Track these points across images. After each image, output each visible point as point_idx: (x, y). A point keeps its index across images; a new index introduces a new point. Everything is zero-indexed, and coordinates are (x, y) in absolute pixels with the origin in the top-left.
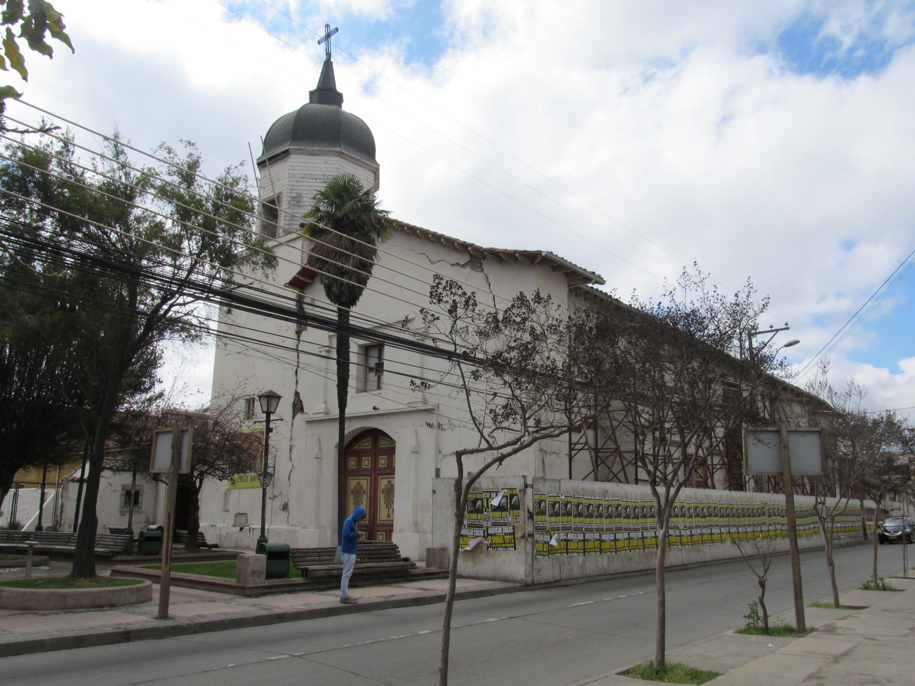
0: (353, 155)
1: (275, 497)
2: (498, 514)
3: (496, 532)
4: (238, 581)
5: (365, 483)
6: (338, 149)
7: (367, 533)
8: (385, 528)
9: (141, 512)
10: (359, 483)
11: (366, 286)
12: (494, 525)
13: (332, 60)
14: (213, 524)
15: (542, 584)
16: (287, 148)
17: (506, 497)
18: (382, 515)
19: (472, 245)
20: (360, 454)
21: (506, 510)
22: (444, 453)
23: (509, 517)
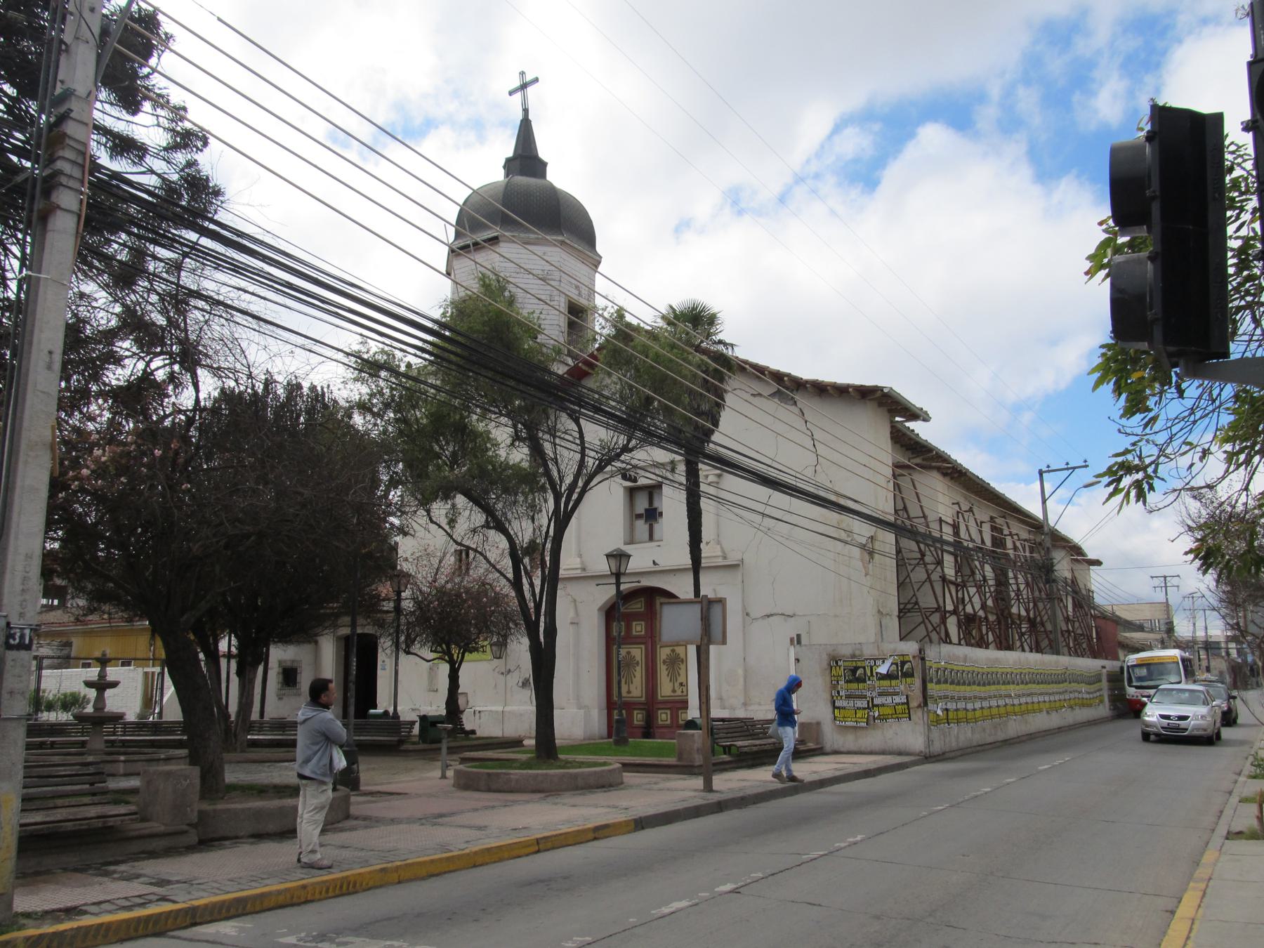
0: (576, 246)
1: (509, 671)
2: (886, 683)
3: (884, 702)
4: (680, 758)
5: (637, 652)
6: (560, 238)
7: (644, 712)
8: (669, 705)
9: (299, 695)
10: (629, 653)
11: (717, 427)
12: (881, 694)
13: (530, 118)
14: (413, 707)
15: (935, 756)
16: (496, 234)
17: (897, 664)
18: (666, 689)
19: (789, 375)
20: (629, 618)
21: (897, 678)
22: (753, 615)
23: (900, 685)
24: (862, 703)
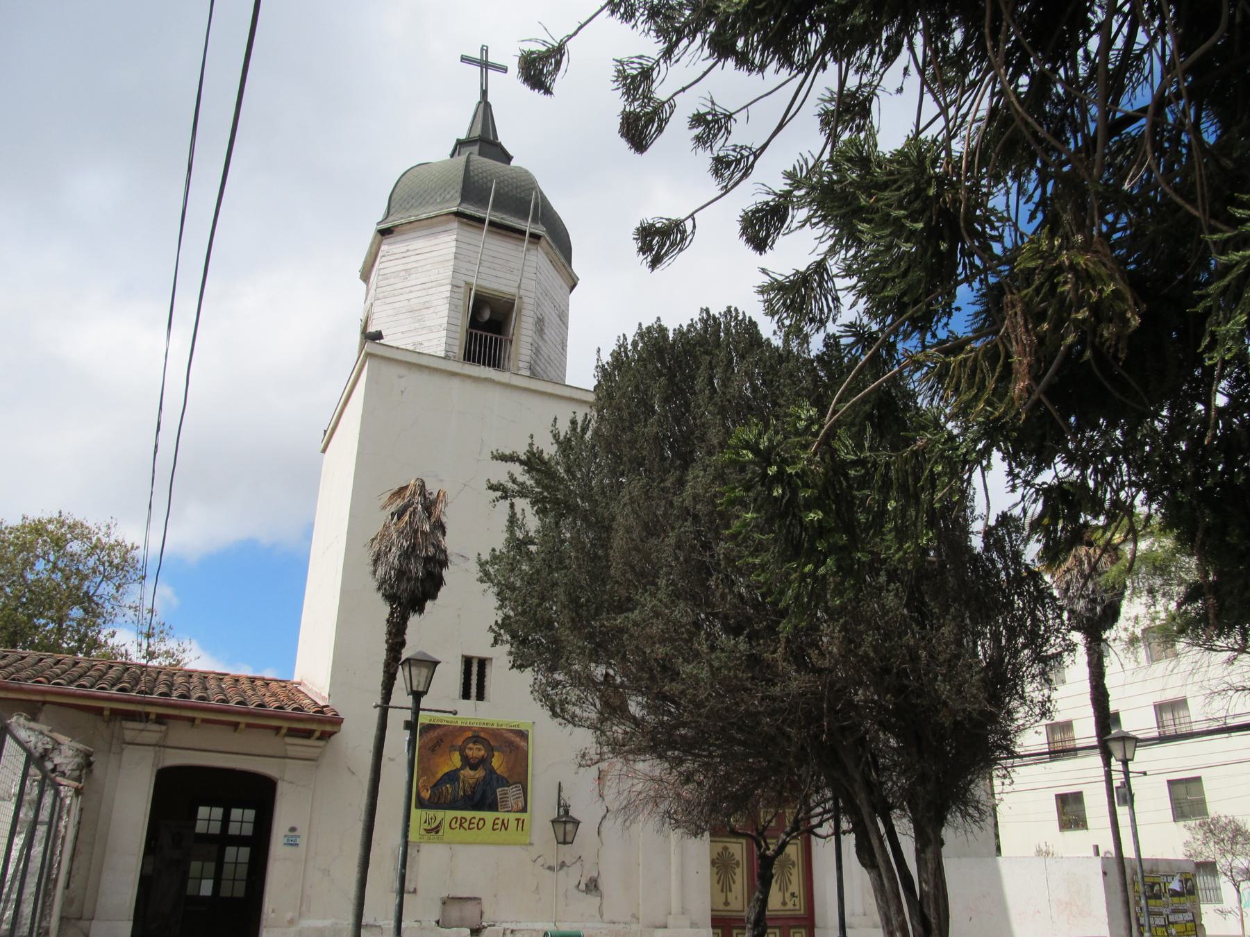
1: (563, 865)
2: (1176, 900)
3: (1177, 919)
8: (779, 923)
10: (726, 849)
12: (1174, 911)
24: (1160, 921)
